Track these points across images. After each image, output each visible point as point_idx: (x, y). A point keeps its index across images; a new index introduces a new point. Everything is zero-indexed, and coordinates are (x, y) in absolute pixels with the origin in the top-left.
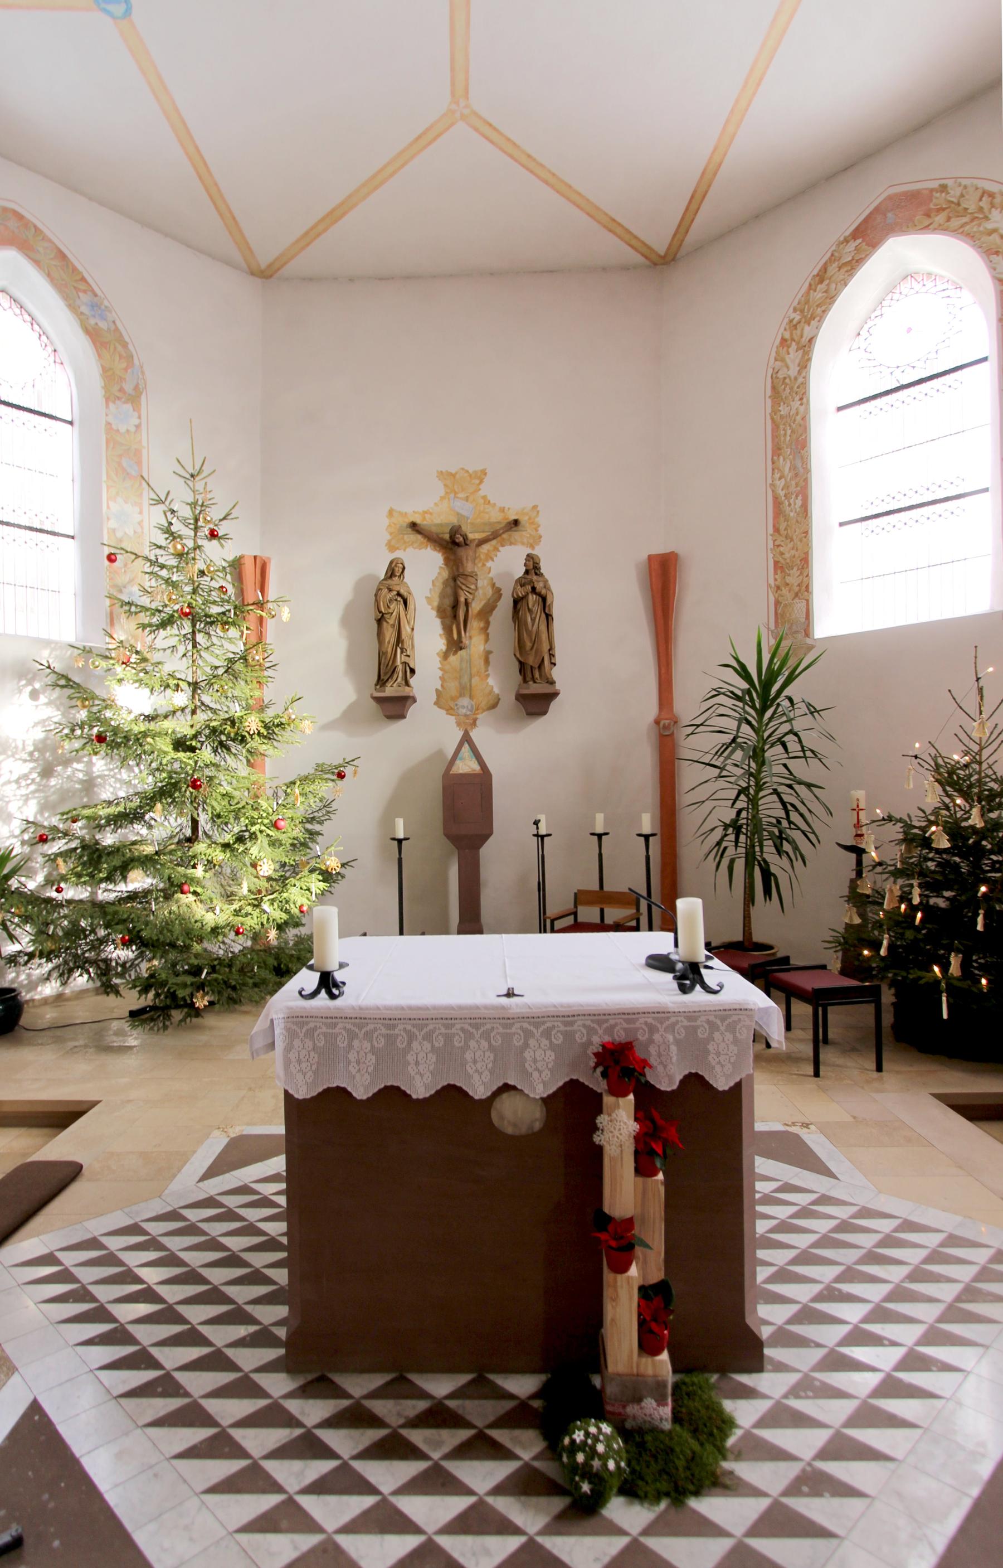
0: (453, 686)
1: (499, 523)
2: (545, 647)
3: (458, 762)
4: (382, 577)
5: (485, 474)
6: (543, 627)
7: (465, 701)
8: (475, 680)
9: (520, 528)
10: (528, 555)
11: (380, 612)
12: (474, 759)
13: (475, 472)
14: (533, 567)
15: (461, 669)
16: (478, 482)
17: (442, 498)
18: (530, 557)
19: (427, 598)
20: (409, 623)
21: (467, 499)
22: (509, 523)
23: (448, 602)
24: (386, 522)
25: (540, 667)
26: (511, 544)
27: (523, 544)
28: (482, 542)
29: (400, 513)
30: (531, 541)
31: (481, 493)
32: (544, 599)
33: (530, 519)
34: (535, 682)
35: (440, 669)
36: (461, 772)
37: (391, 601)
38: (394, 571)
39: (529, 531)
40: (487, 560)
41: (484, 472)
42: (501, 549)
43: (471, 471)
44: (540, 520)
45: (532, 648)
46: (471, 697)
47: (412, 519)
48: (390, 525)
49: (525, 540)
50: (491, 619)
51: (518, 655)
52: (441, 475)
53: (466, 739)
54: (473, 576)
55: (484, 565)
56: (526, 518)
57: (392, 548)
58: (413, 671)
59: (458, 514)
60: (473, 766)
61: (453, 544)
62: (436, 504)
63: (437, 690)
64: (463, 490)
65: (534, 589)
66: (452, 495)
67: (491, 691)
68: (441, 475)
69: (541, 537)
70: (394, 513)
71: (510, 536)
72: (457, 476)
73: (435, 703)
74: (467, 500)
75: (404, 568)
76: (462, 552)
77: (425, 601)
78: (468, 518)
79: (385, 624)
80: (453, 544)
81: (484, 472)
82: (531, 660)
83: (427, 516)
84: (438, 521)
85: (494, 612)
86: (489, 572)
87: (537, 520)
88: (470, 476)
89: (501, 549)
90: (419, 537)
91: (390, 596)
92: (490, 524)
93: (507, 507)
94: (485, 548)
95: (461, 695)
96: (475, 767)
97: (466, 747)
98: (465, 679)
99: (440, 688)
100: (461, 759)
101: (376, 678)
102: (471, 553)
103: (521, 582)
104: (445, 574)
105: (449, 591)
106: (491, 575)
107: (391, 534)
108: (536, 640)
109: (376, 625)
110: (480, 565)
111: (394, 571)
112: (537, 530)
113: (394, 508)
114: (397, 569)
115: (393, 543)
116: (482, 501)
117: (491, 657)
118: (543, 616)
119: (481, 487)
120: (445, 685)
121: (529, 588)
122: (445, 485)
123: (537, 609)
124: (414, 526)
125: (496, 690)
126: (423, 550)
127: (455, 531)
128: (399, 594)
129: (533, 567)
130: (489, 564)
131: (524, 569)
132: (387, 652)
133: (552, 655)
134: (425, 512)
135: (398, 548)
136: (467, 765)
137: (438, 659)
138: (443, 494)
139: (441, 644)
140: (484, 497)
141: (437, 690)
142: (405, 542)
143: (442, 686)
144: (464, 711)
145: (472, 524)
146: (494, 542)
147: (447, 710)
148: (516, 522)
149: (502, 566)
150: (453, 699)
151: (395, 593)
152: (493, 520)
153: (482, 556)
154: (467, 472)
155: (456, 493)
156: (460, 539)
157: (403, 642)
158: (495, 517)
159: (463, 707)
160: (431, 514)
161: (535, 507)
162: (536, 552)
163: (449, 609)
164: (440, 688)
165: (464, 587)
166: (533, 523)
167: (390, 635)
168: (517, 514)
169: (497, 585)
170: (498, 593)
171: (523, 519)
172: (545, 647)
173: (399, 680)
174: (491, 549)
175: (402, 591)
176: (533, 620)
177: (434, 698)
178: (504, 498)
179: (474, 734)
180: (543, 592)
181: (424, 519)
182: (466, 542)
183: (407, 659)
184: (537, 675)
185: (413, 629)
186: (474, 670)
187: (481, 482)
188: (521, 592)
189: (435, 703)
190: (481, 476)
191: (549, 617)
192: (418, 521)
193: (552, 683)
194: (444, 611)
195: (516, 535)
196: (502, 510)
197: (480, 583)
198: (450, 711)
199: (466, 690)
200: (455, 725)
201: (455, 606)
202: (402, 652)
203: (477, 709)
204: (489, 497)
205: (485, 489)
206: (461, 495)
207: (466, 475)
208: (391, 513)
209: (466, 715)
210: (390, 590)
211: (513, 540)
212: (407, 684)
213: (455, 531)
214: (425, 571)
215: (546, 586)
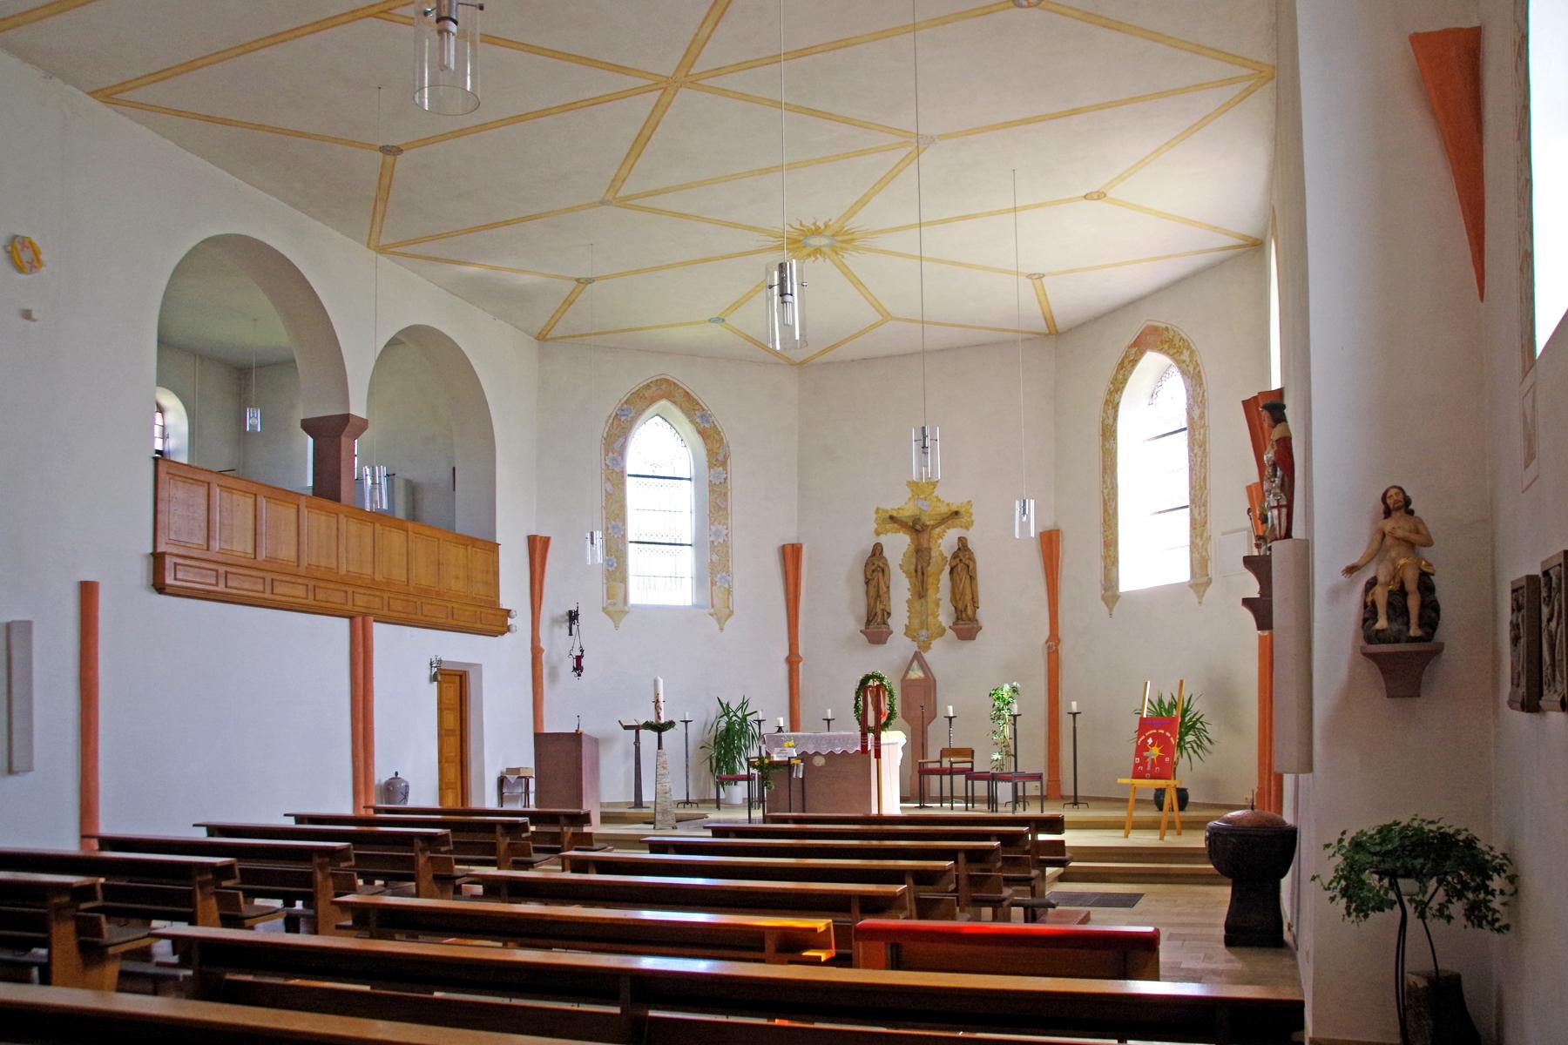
0: (916, 622)
2: (968, 597)
7: (924, 632)
14: (962, 542)
28: (934, 527)
38: (877, 550)
44: (973, 510)
57: (878, 534)
61: (916, 527)
80: (916, 527)
82: (960, 606)
84: (907, 513)
103: (955, 556)
108: (963, 593)
111: (877, 550)
124: (892, 518)
127: (916, 520)
129: (962, 542)
136: (916, 674)
139: (908, 595)
148: (957, 513)
149: (946, 543)
158: (944, 509)
171: (962, 510)
178: (950, 497)
182: (925, 527)
191: (972, 578)
195: (957, 522)
197: (933, 554)
199: (924, 625)
205: (937, 492)
208: (878, 510)
214: (898, 546)
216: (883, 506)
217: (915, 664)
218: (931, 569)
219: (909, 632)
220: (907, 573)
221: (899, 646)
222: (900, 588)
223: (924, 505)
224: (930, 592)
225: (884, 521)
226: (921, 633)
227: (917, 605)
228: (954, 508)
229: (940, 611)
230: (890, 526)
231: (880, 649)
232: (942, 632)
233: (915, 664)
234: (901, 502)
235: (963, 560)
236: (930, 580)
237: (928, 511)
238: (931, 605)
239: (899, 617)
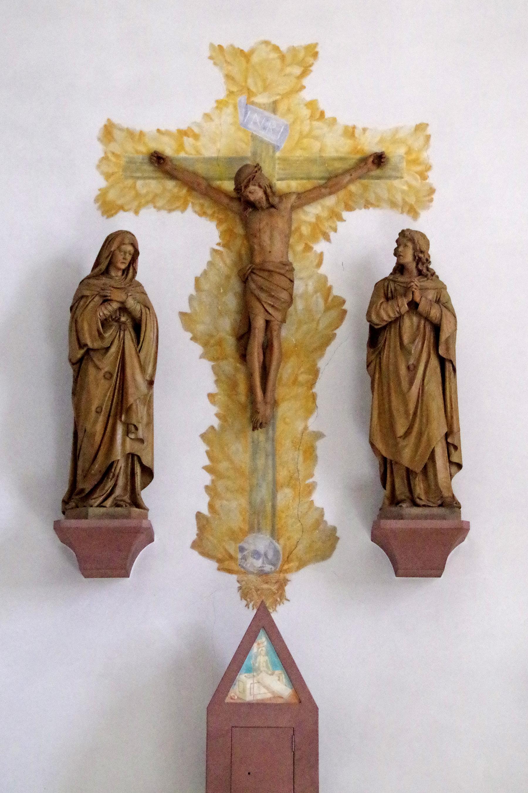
0: (235, 508)
1: (341, 159)
2: (438, 428)
3: (243, 677)
4: (88, 271)
5: (315, 55)
6: (434, 387)
7: (261, 542)
8: (285, 496)
9: (388, 170)
10: (403, 234)
11: (81, 345)
12: (279, 672)
13: (293, 50)
15: (254, 471)
16: (297, 71)
17: (220, 105)
18: (406, 238)
19: (182, 314)
20: (143, 369)
21: (274, 108)
22: (364, 160)
23: (227, 325)
24: (98, 150)
25: (425, 469)
26: (368, 205)
27: (393, 204)
28: (306, 198)
29: (130, 134)
30: (412, 200)
31: (306, 95)
32: (437, 329)
33: (409, 152)
34: (415, 504)
35: (206, 468)
36: (249, 698)
37: (105, 323)
38: (117, 258)
39: (407, 178)
40: (314, 238)
41: (312, 51)
42: (345, 214)
43: (284, 48)
45: (407, 433)
46: (274, 534)
47: (154, 146)
48: (105, 158)
49: (399, 198)
50: (321, 364)
51: (380, 446)
52: (219, 54)
53: (263, 623)
54: (287, 271)
55: (308, 248)
56: (402, 151)
57: (108, 208)
58: (148, 473)
59: (254, 138)
60: (278, 686)
62: (207, 117)
63: (199, 515)
64: (266, 88)
65: (414, 305)
66: (242, 99)
67: (320, 521)
68: (219, 54)
69: (432, 191)
70: (117, 134)
71: (366, 188)
72: (255, 59)
73: (195, 545)
74: (274, 111)
75: (136, 254)
76: (261, 221)
77: (177, 322)
78: (276, 148)
79: (92, 371)
81: (312, 51)
82: (406, 456)
83: (188, 141)
84: (210, 152)
85: (330, 349)
86: (319, 264)
87: (424, 155)
88: (283, 58)
89: (345, 214)
90: (170, 184)
91: (105, 311)
92: (323, 161)
93: (360, 126)
94: (312, 212)
95: (253, 528)
96: (278, 686)
97: (262, 642)
98: (264, 492)
99: (205, 511)
100: (250, 670)
101: (65, 488)
102: (280, 223)
103: (386, 291)
104: (226, 264)
105: (231, 302)
106: (322, 270)
107: (107, 176)
108: (419, 413)
109: (70, 371)
110: (300, 248)
111: (117, 258)
112: (424, 177)
113: (116, 120)
114: (120, 257)
115: (112, 195)
116: (306, 112)
117: (320, 444)
118: (434, 362)
119: (305, 81)
120: (218, 504)
121: (403, 304)
122: (229, 77)
123: (420, 348)
124: (158, 160)
125: (330, 519)
126: (177, 215)
127: (247, 175)
128: (123, 309)
129: (412, 259)
130: (320, 246)
131: (393, 261)
132: (93, 435)
133: (452, 447)
134: (183, 133)
135: (122, 208)
136: (261, 684)
137: (203, 447)
138: (222, 95)
139: (208, 416)
140: (312, 105)
141: (199, 515)
142: (138, 195)
143: (211, 506)
144: (258, 563)
145: (284, 160)
146: (330, 201)
147: (219, 561)
148: (379, 160)
149: (346, 250)
150: (235, 536)
151: (115, 306)
152: (330, 152)
153: (305, 230)
154: (276, 48)
155: (250, 93)
156: (256, 194)
157: (129, 410)
158: (334, 146)
159: (256, 554)
160: (196, 137)
161: (421, 128)
162: (423, 224)
163: (230, 343)
164: (205, 511)
165: (263, 296)
166: (416, 162)
167: (100, 391)
168: (381, 141)
169: (336, 292)
170: (336, 307)
171: (396, 153)
172: (438, 428)
173: (118, 491)
174: (325, 214)
175: (131, 303)
176: (412, 369)
177: (192, 533)
179: (280, 616)
180: (434, 313)
181: (181, 147)
182: (272, 201)
183: (136, 448)
184: (419, 488)
185: (151, 383)
186: (283, 474)
187: (305, 72)
188: (387, 313)
189: (195, 545)
190: (305, 58)
192: (168, 149)
193: (451, 505)
194: (220, 343)
195: (379, 187)
196: (350, 132)
197: (299, 287)
198: (226, 563)
199: (263, 517)
200: (237, 596)
201: (243, 337)
202: (127, 432)
203: (288, 560)
204: (322, 106)
205: (315, 88)
206: (262, 99)
207: (273, 55)
208: (108, 132)
209: (262, 573)
210: (106, 300)
211: (372, 197)
212: (136, 502)
213: (247, 175)
215: (442, 301)
216: (124, 119)
217: (262, 646)
218: (288, 335)
219: (206, 539)
220: (210, 346)
221: (176, 592)
222: (184, 395)
223: (271, 129)
224: (285, 409)
225: (130, 168)
226: (255, 547)
227: (239, 451)
228: (371, 145)
229: (319, 475)
230: (153, 184)
231: (109, 594)
232: (325, 544)
233: (262, 646)
234: (189, 110)
235: (408, 321)
236: (286, 371)
237: (287, 150)
238: (289, 456)
239: (179, 488)
